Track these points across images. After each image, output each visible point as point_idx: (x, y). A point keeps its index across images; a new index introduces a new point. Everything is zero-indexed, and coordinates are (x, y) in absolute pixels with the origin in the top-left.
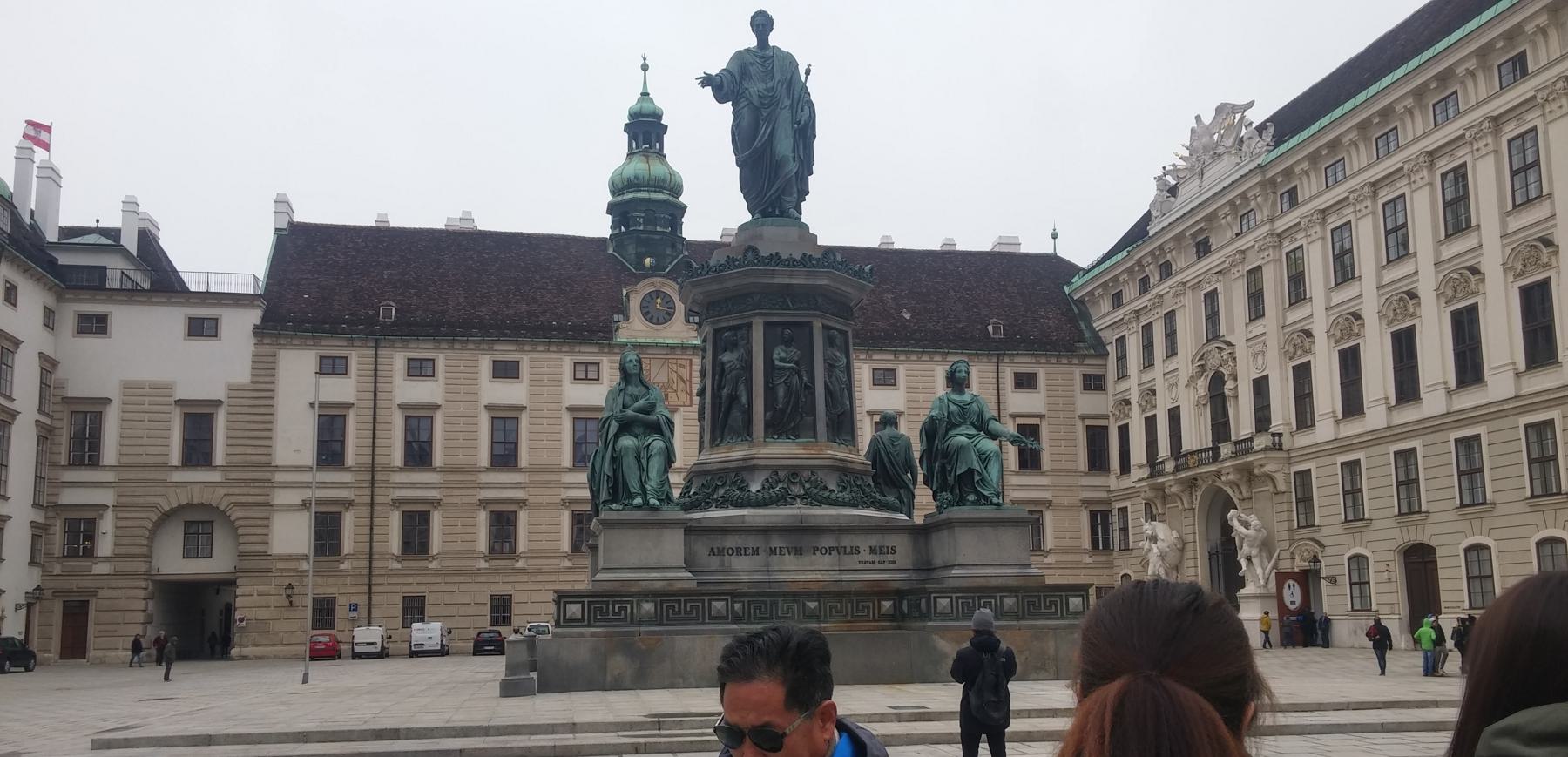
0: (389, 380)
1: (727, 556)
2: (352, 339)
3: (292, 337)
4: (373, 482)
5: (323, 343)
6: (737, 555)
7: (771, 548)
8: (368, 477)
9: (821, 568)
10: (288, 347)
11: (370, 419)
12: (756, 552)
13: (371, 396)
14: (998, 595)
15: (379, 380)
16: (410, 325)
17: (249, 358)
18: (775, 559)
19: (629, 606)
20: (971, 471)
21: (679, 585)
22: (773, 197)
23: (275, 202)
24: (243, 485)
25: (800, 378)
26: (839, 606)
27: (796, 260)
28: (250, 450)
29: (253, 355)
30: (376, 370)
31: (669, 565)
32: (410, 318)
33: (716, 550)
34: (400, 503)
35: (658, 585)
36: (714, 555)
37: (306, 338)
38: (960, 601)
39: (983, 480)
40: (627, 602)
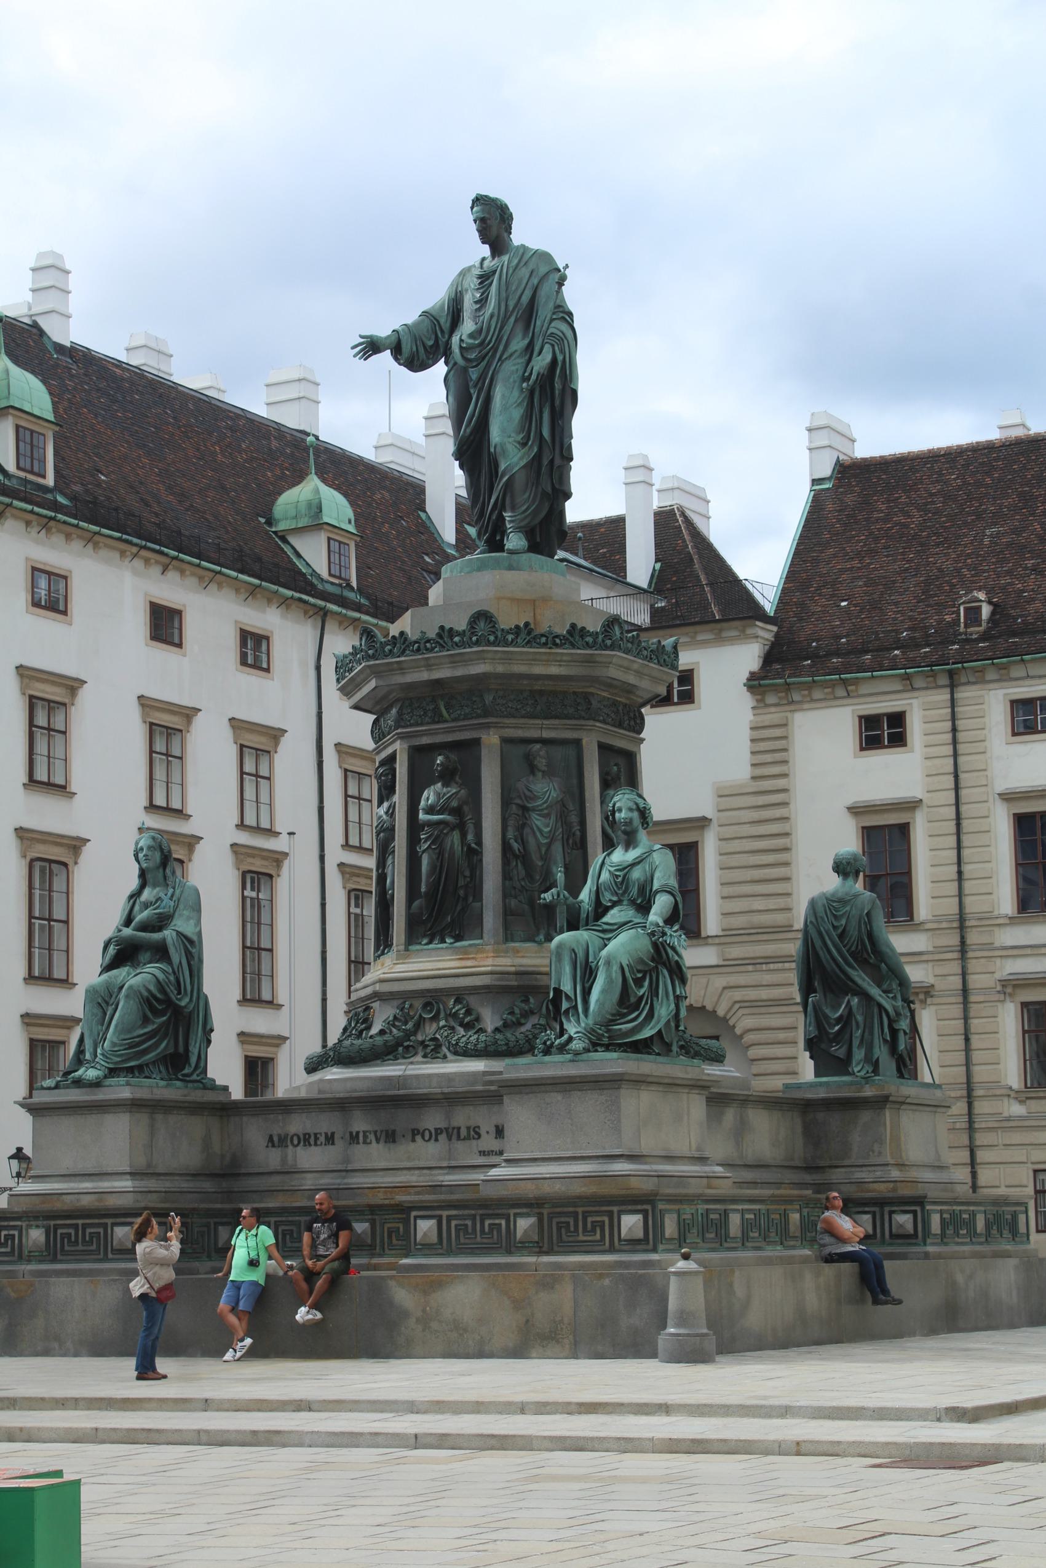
0: (980, 747)
1: (291, 1147)
2: (907, 677)
3: (810, 686)
4: (963, 947)
5: (864, 689)
6: (305, 1145)
7: (351, 1133)
8: (954, 940)
9: (422, 1164)
10: (806, 706)
11: (951, 827)
12: (330, 1139)
13: (949, 782)
14: (512, 1212)
15: (961, 748)
16: (1014, 634)
17: (745, 734)
18: (359, 1149)
19: (16, 1233)
20: (558, 991)
21: (112, 1202)
22: (494, 517)
23: (810, 430)
24: (750, 968)
25: (463, 835)
26: (401, 1230)
27: (428, 641)
28: (758, 904)
29: (751, 728)
30: (954, 730)
31: (110, 1170)
32: (1015, 618)
33: (276, 1139)
34: (1015, 986)
35: (86, 1201)
36: (273, 1146)
37: (833, 685)
38: (453, 1223)
39: (575, 1007)
40: (14, 1227)
